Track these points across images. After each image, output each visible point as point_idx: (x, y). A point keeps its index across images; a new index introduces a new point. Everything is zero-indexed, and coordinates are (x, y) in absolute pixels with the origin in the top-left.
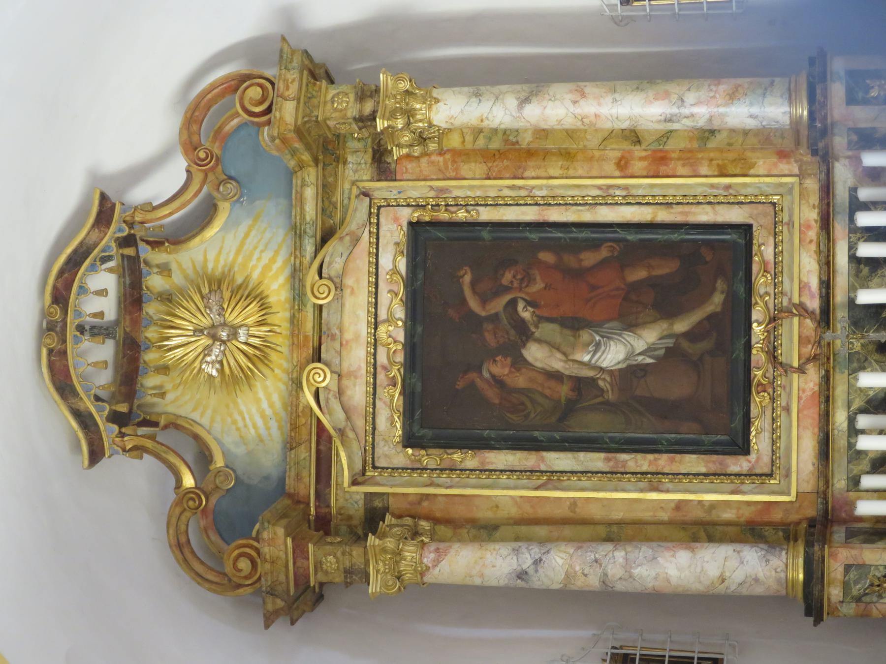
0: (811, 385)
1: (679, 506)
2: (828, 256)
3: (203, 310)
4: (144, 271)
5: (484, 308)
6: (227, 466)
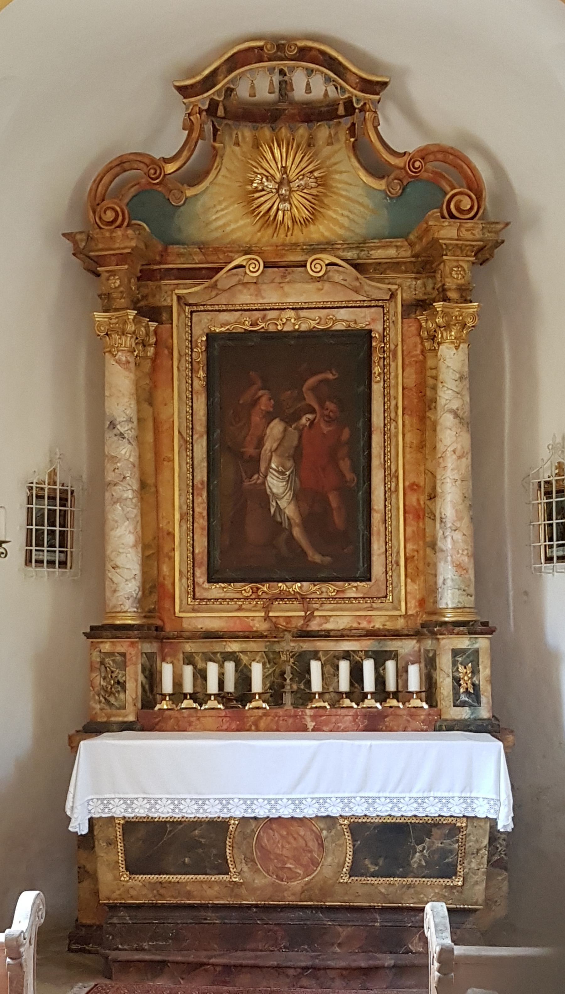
0: (257, 625)
1: (171, 535)
2: (348, 636)
3: (302, 173)
4: (331, 123)
5: (309, 389)
6: (186, 199)
